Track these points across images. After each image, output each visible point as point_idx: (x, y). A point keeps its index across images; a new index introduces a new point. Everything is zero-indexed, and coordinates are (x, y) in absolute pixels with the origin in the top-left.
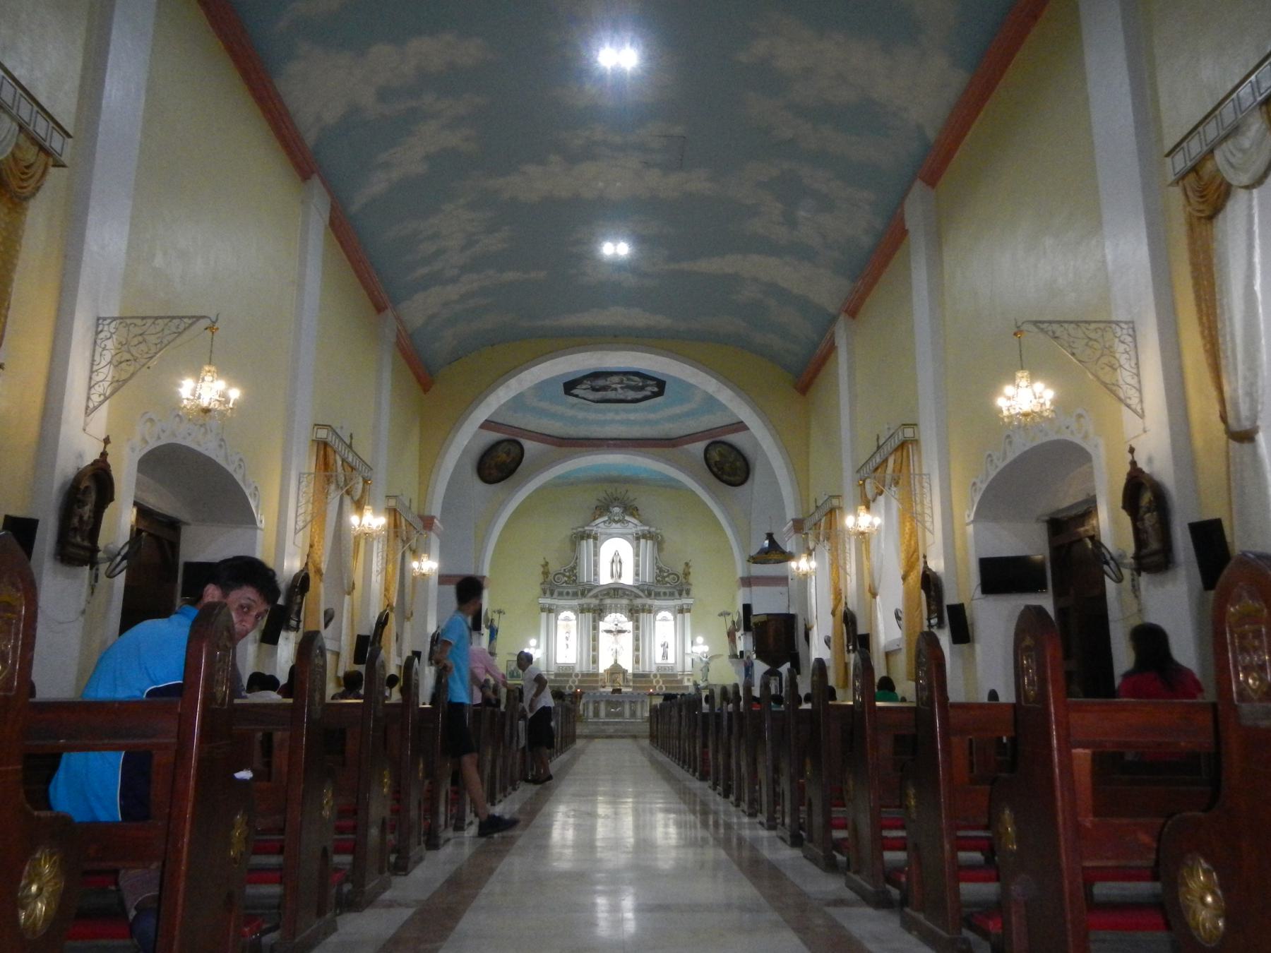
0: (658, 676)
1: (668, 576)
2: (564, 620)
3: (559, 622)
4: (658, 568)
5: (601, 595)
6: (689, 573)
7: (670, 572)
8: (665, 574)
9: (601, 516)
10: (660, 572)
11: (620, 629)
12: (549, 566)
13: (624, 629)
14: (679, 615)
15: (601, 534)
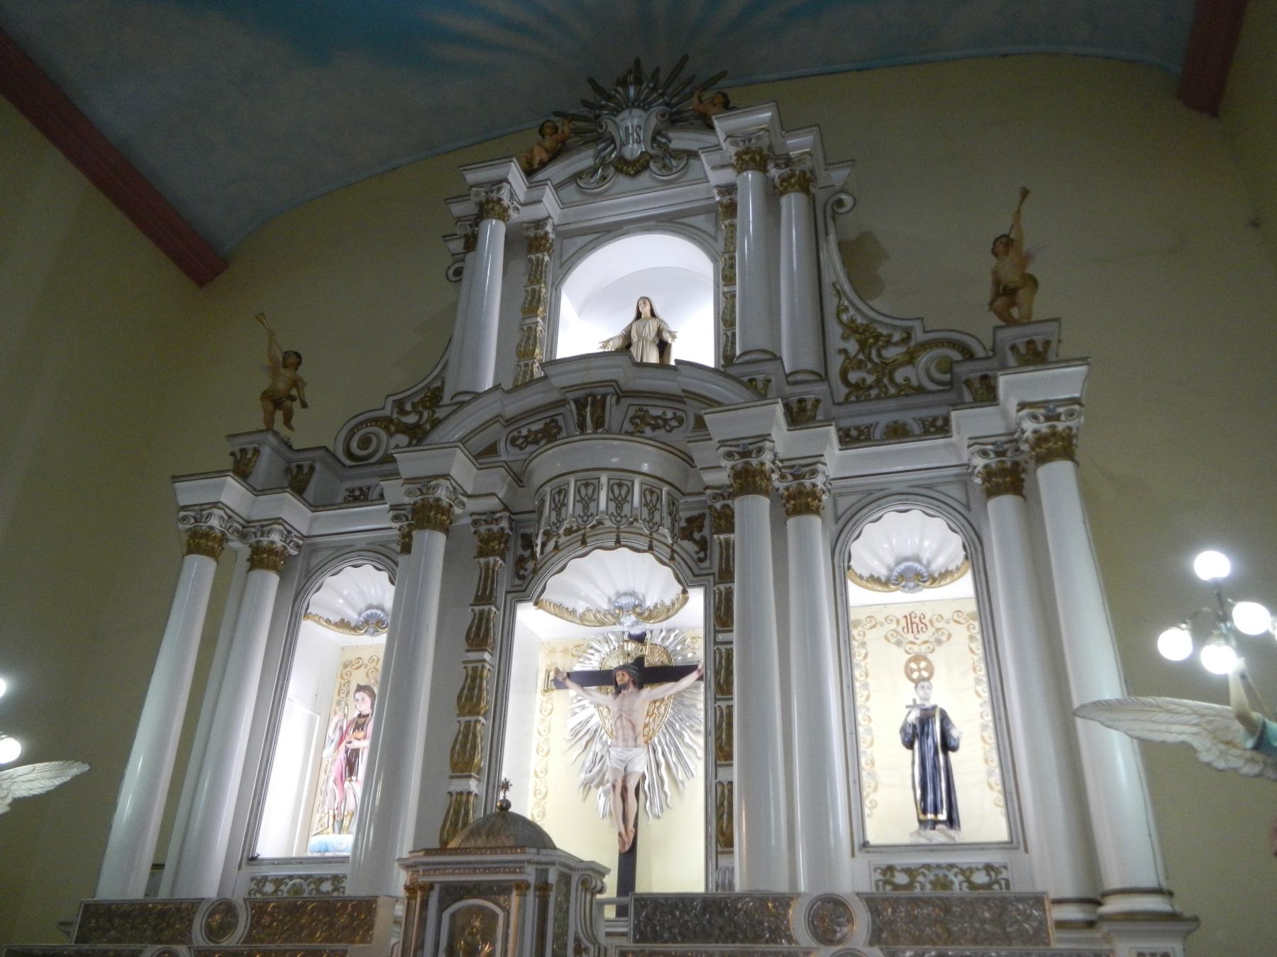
0: (860, 926)
1: (910, 359)
2: (356, 629)
3: (307, 628)
4: (852, 329)
5: (513, 442)
6: (1032, 282)
7: (919, 336)
8: (891, 353)
9: (556, 154)
10: (863, 345)
11: (653, 659)
12: (302, 372)
13: (678, 661)
14: (992, 504)
15: (566, 234)
